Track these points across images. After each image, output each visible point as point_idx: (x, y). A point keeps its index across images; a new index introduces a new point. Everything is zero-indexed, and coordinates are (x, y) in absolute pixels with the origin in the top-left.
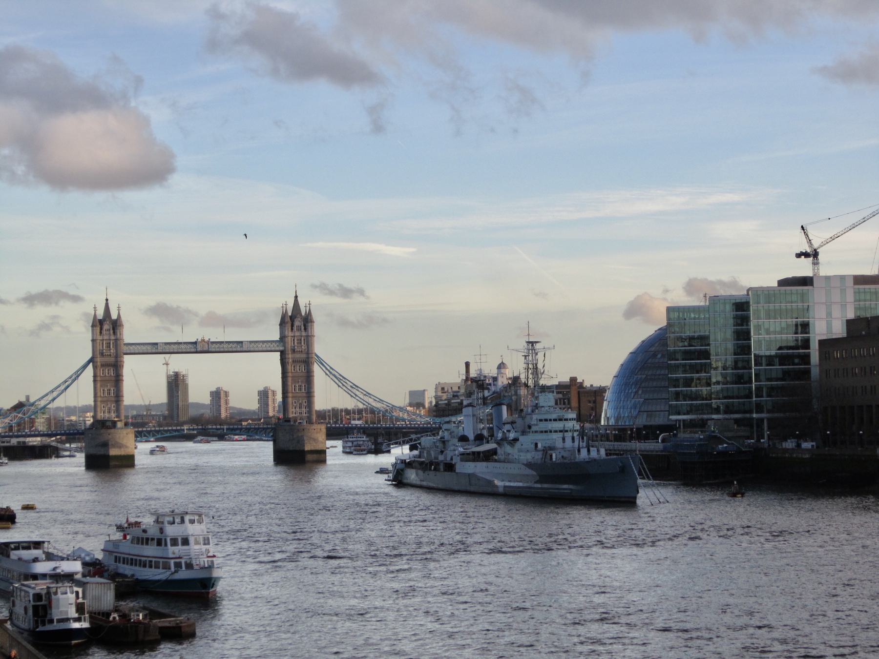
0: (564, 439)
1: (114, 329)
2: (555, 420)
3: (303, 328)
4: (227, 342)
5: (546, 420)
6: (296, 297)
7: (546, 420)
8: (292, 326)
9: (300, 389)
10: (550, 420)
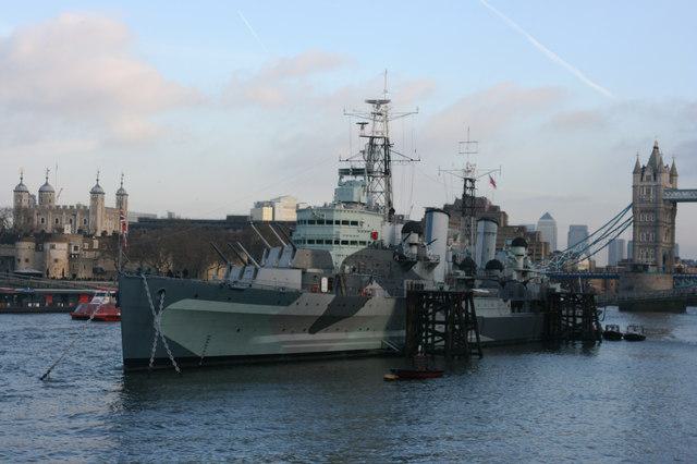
1: (655, 175)
2: (311, 222)
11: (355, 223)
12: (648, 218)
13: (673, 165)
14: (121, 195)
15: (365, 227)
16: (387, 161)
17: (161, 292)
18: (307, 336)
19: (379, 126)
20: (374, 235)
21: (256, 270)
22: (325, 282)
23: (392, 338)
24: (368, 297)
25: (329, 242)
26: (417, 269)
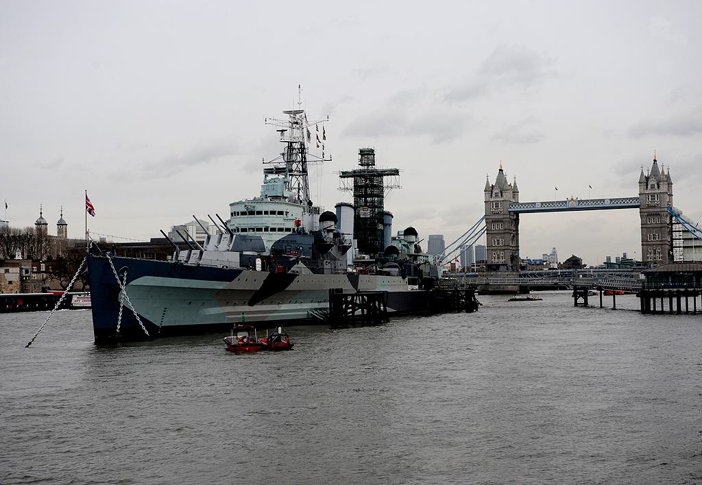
1: (501, 192)
2: (243, 213)
3: (656, 186)
6: (655, 161)
8: (647, 185)
11: (281, 213)
12: (498, 227)
13: (515, 183)
14: (62, 224)
15: (290, 216)
16: (304, 162)
17: (123, 272)
18: (247, 308)
19: (297, 133)
20: (298, 223)
21: (201, 253)
22: (259, 262)
23: (316, 309)
24: (294, 276)
25: (260, 230)
26: (333, 251)
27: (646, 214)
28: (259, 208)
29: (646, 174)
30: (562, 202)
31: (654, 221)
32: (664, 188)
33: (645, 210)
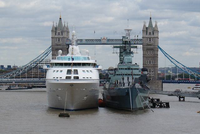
0: (123, 79)
3: (152, 33)
4: (115, 40)
5: (122, 69)
7: (122, 69)
9: (150, 63)
10: (124, 69)
27: (146, 49)
28: (131, 67)
29: (147, 26)
30: (98, 40)
31: (150, 53)
32: (155, 35)
33: (145, 47)
